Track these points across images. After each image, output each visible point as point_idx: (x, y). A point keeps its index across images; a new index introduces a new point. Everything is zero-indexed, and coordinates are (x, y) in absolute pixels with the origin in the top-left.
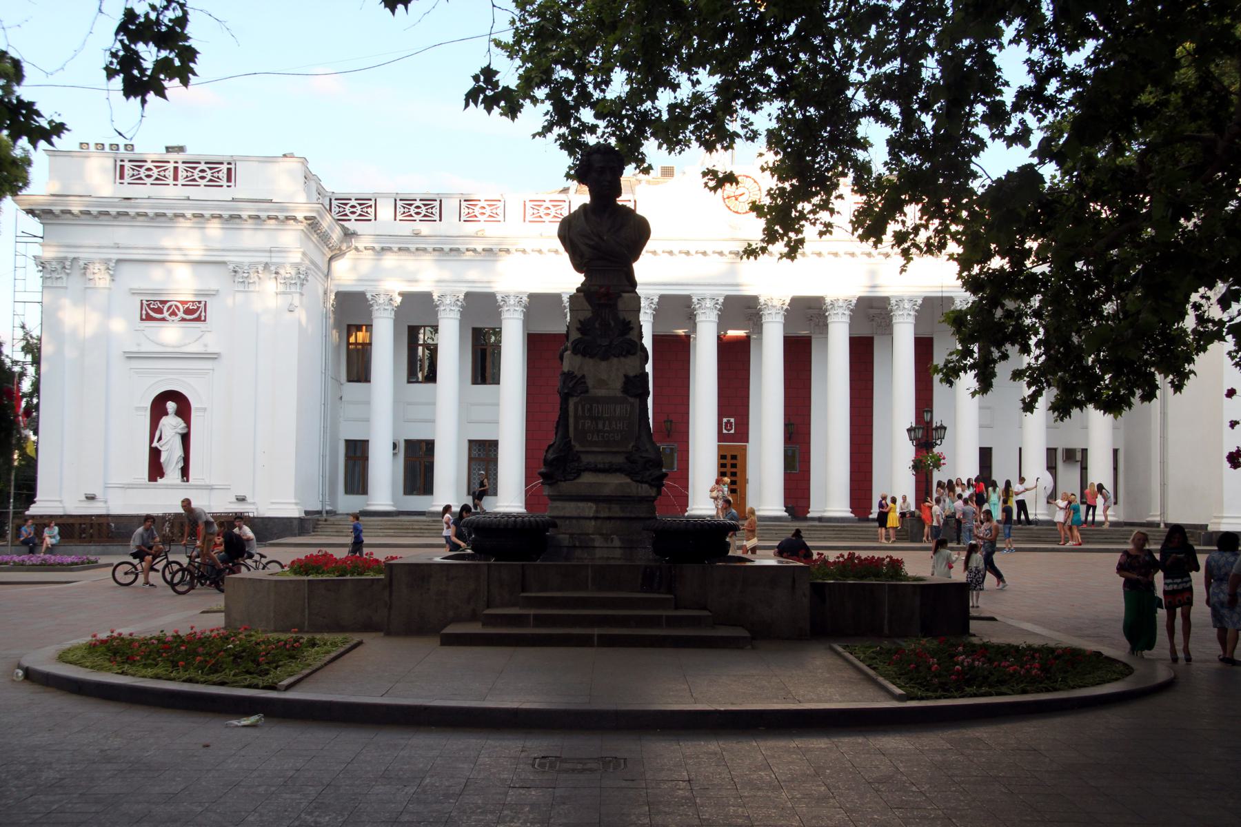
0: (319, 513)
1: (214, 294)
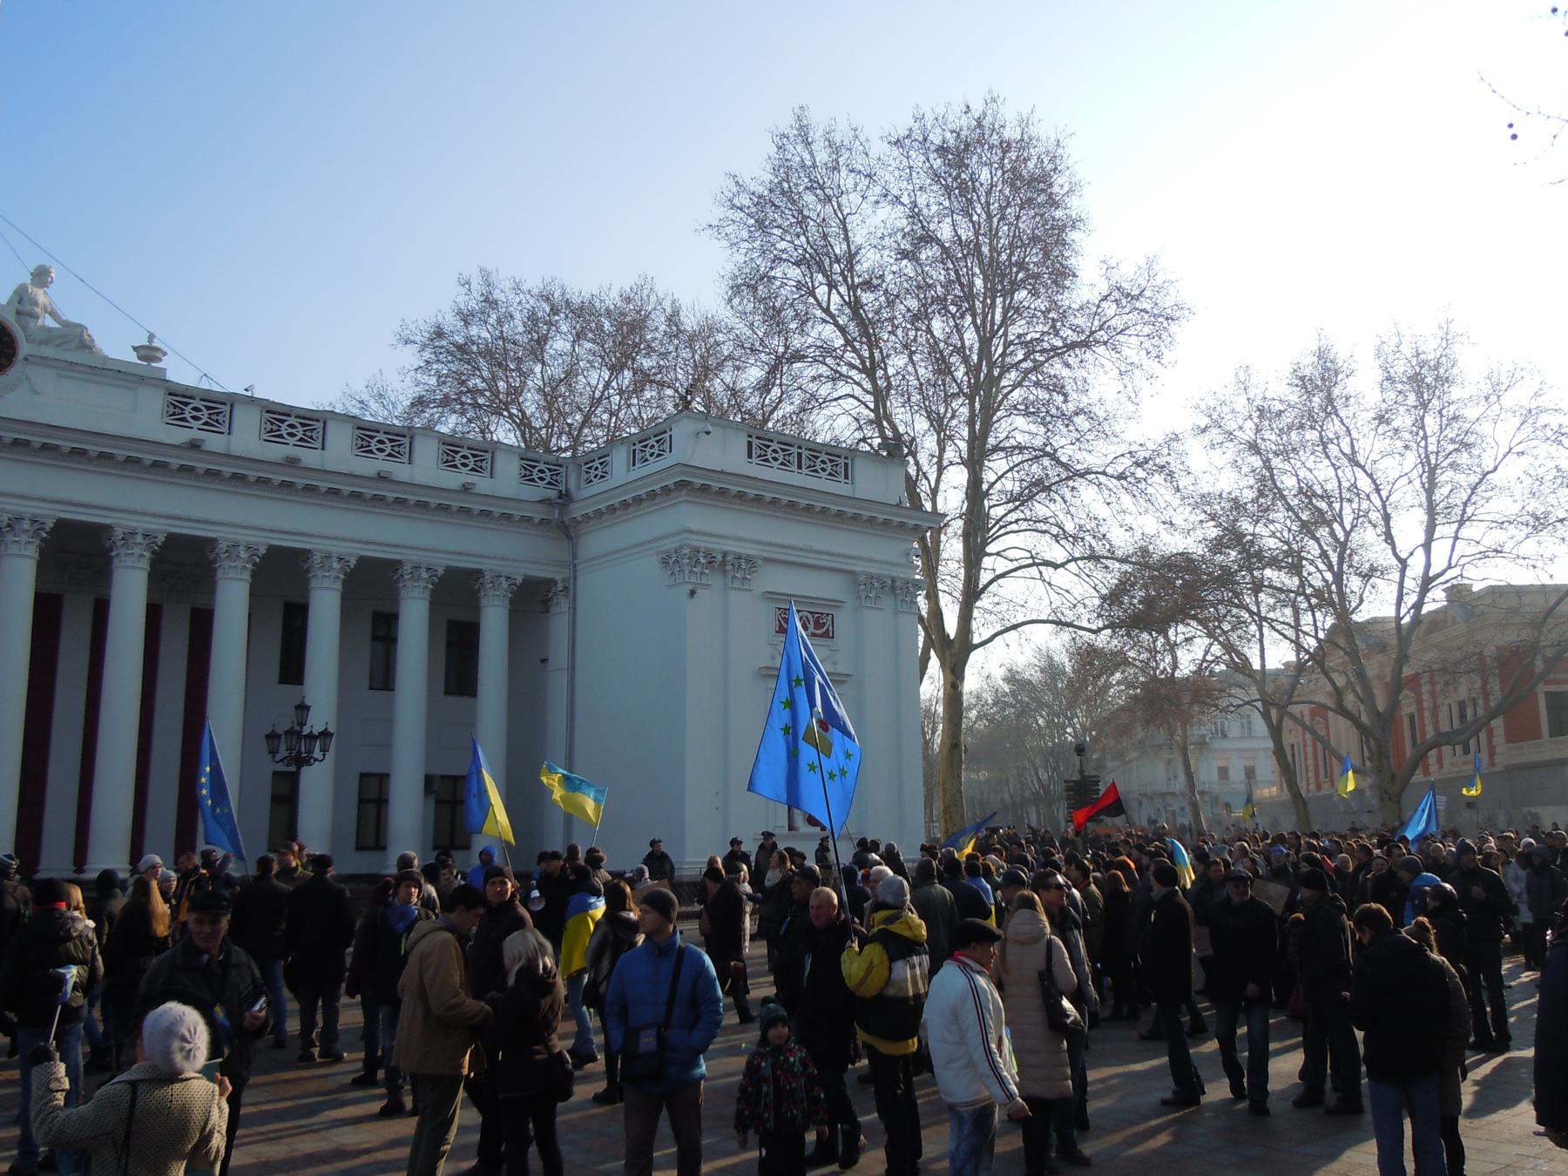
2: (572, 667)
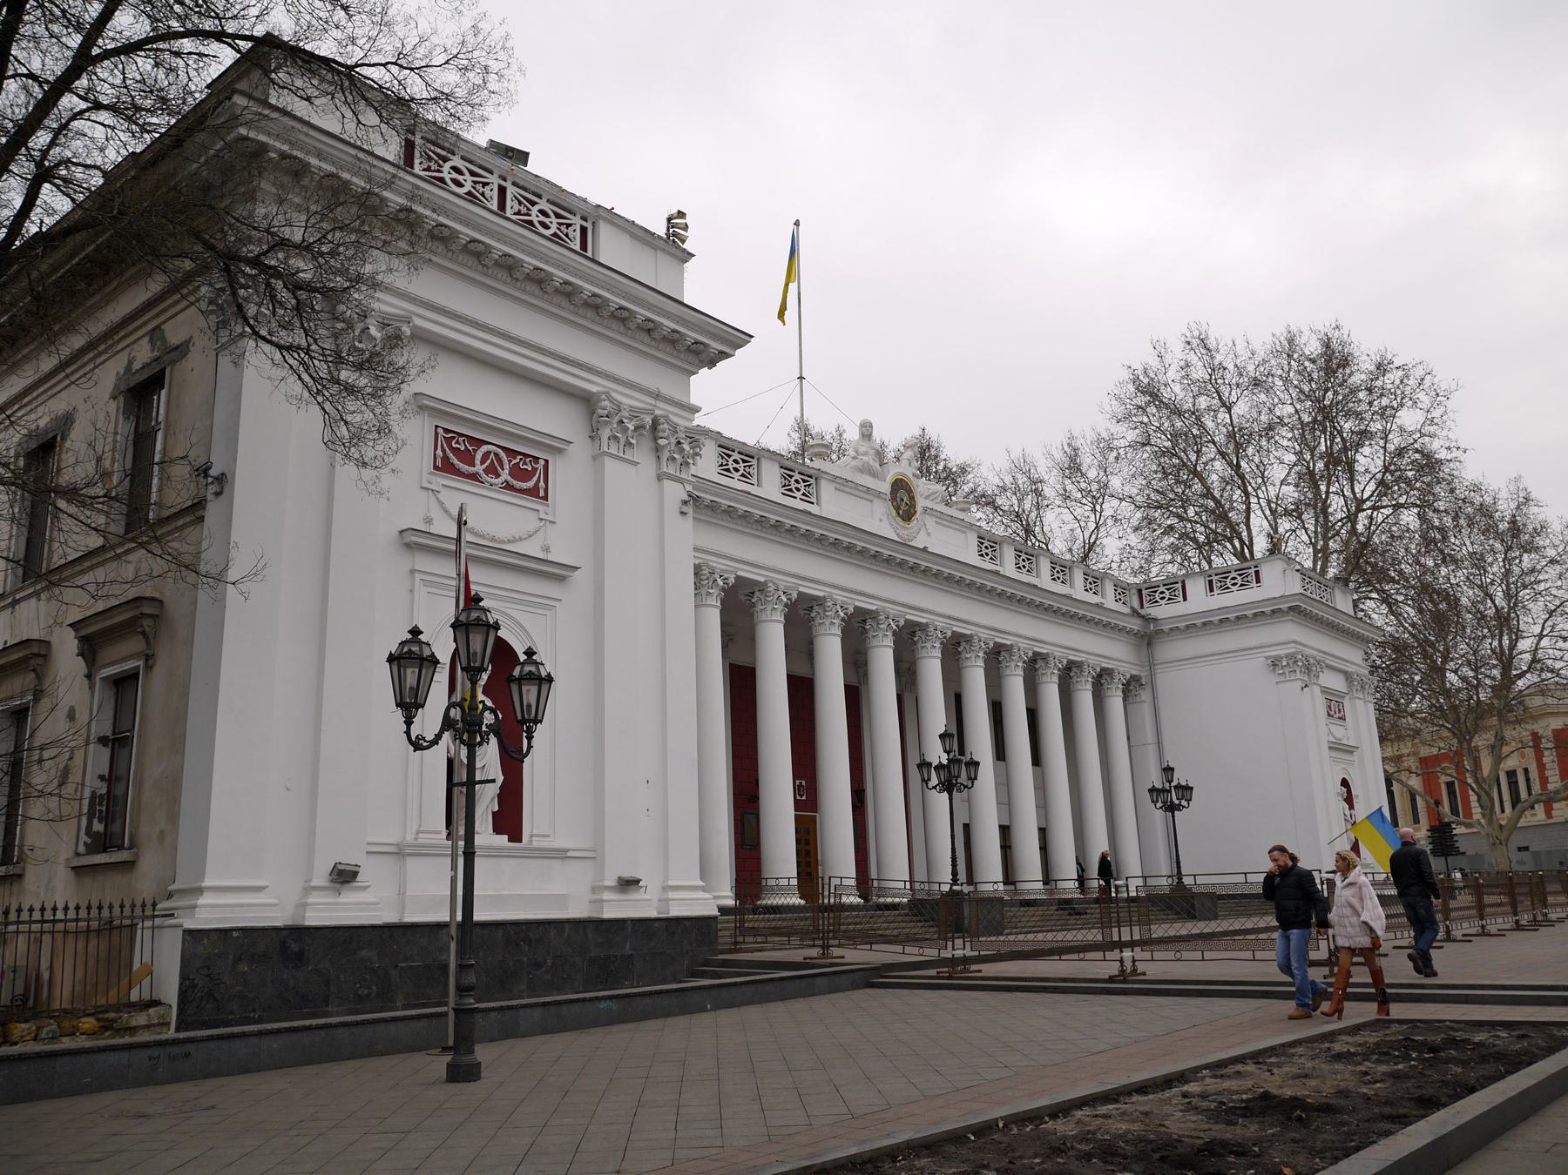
1: (557, 447)
2: (1159, 743)
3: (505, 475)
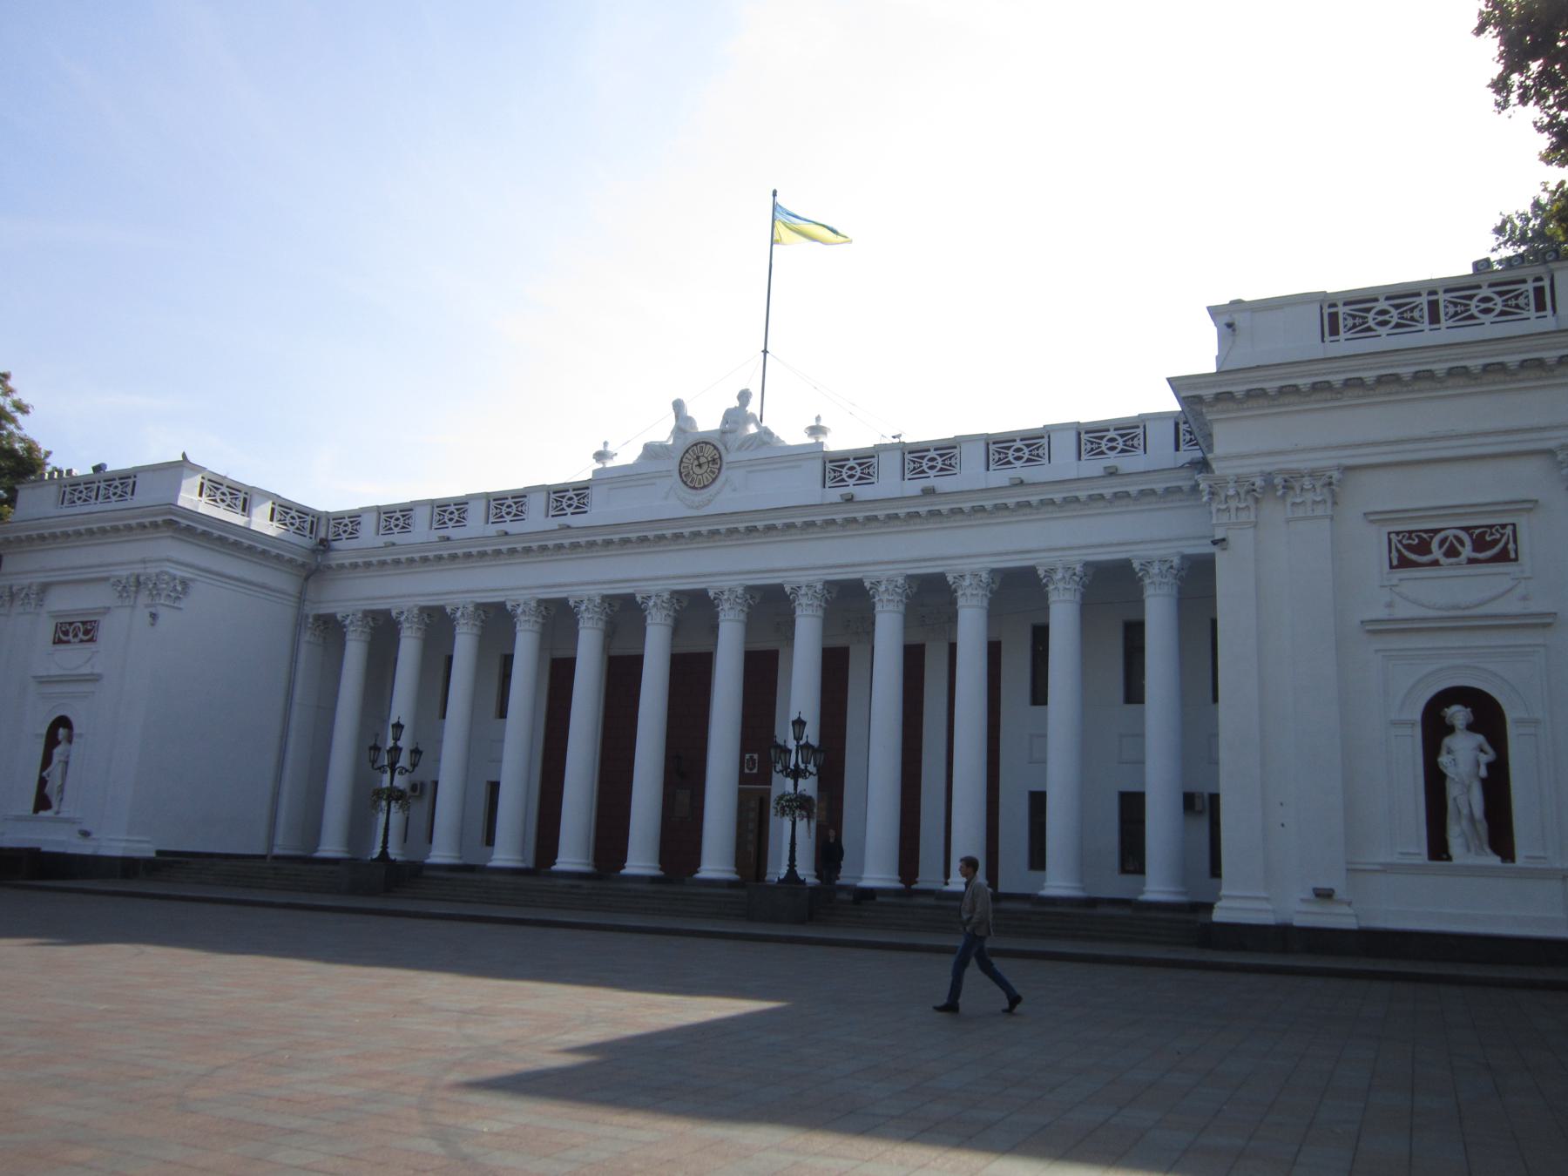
0: (263, 857)
3: (81, 636)
